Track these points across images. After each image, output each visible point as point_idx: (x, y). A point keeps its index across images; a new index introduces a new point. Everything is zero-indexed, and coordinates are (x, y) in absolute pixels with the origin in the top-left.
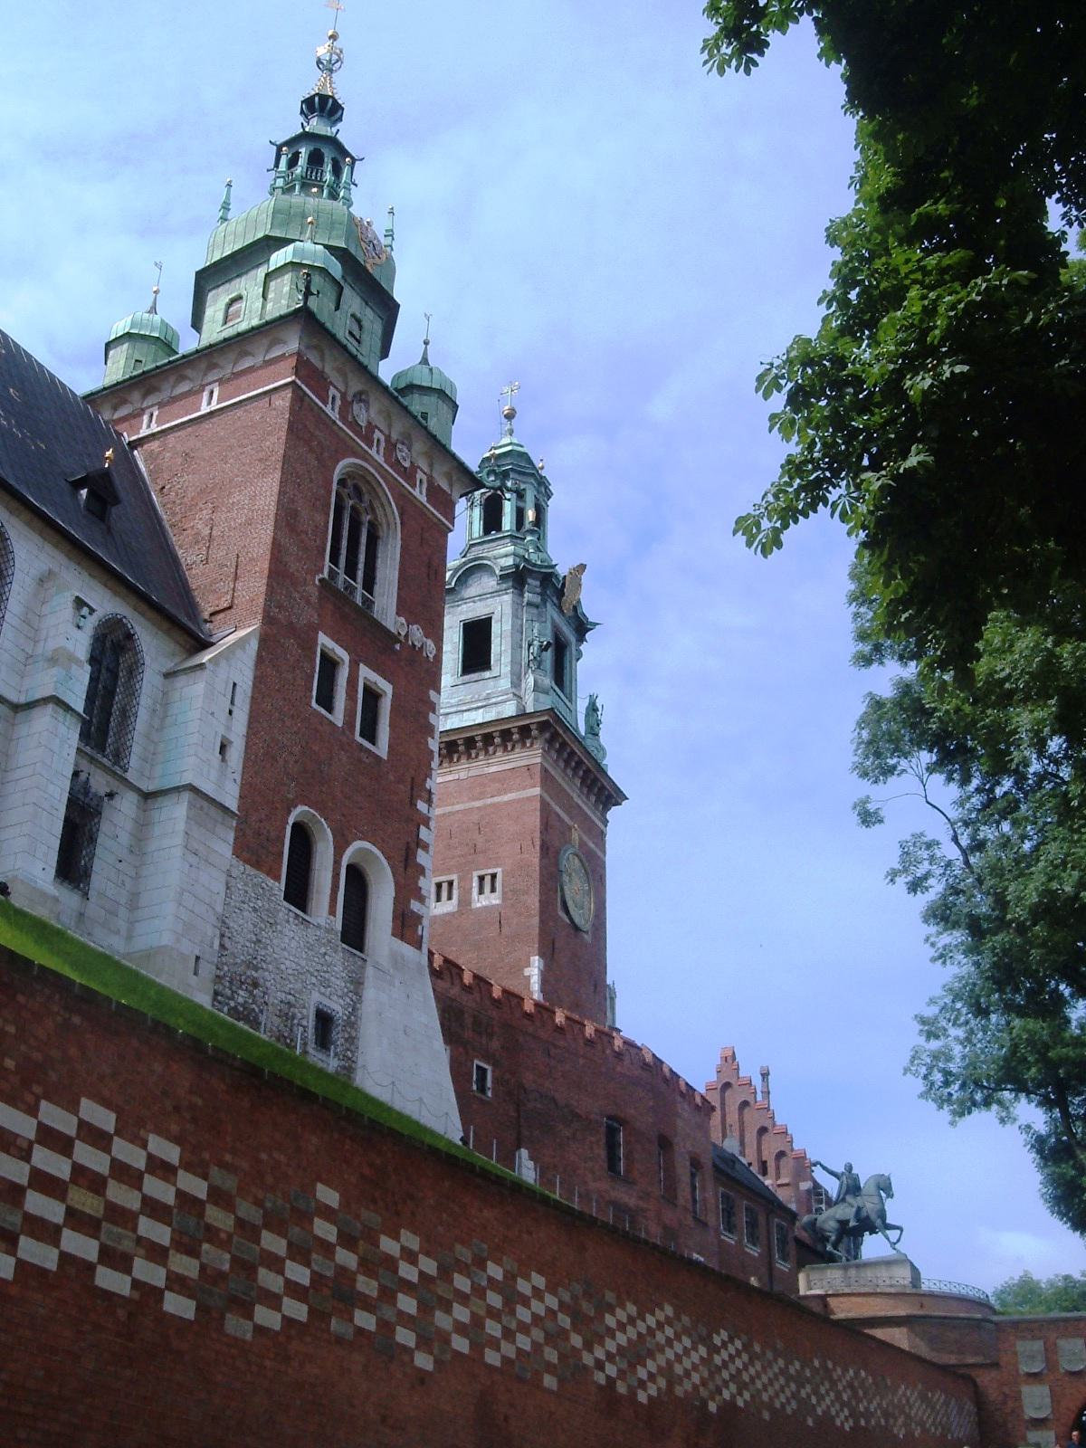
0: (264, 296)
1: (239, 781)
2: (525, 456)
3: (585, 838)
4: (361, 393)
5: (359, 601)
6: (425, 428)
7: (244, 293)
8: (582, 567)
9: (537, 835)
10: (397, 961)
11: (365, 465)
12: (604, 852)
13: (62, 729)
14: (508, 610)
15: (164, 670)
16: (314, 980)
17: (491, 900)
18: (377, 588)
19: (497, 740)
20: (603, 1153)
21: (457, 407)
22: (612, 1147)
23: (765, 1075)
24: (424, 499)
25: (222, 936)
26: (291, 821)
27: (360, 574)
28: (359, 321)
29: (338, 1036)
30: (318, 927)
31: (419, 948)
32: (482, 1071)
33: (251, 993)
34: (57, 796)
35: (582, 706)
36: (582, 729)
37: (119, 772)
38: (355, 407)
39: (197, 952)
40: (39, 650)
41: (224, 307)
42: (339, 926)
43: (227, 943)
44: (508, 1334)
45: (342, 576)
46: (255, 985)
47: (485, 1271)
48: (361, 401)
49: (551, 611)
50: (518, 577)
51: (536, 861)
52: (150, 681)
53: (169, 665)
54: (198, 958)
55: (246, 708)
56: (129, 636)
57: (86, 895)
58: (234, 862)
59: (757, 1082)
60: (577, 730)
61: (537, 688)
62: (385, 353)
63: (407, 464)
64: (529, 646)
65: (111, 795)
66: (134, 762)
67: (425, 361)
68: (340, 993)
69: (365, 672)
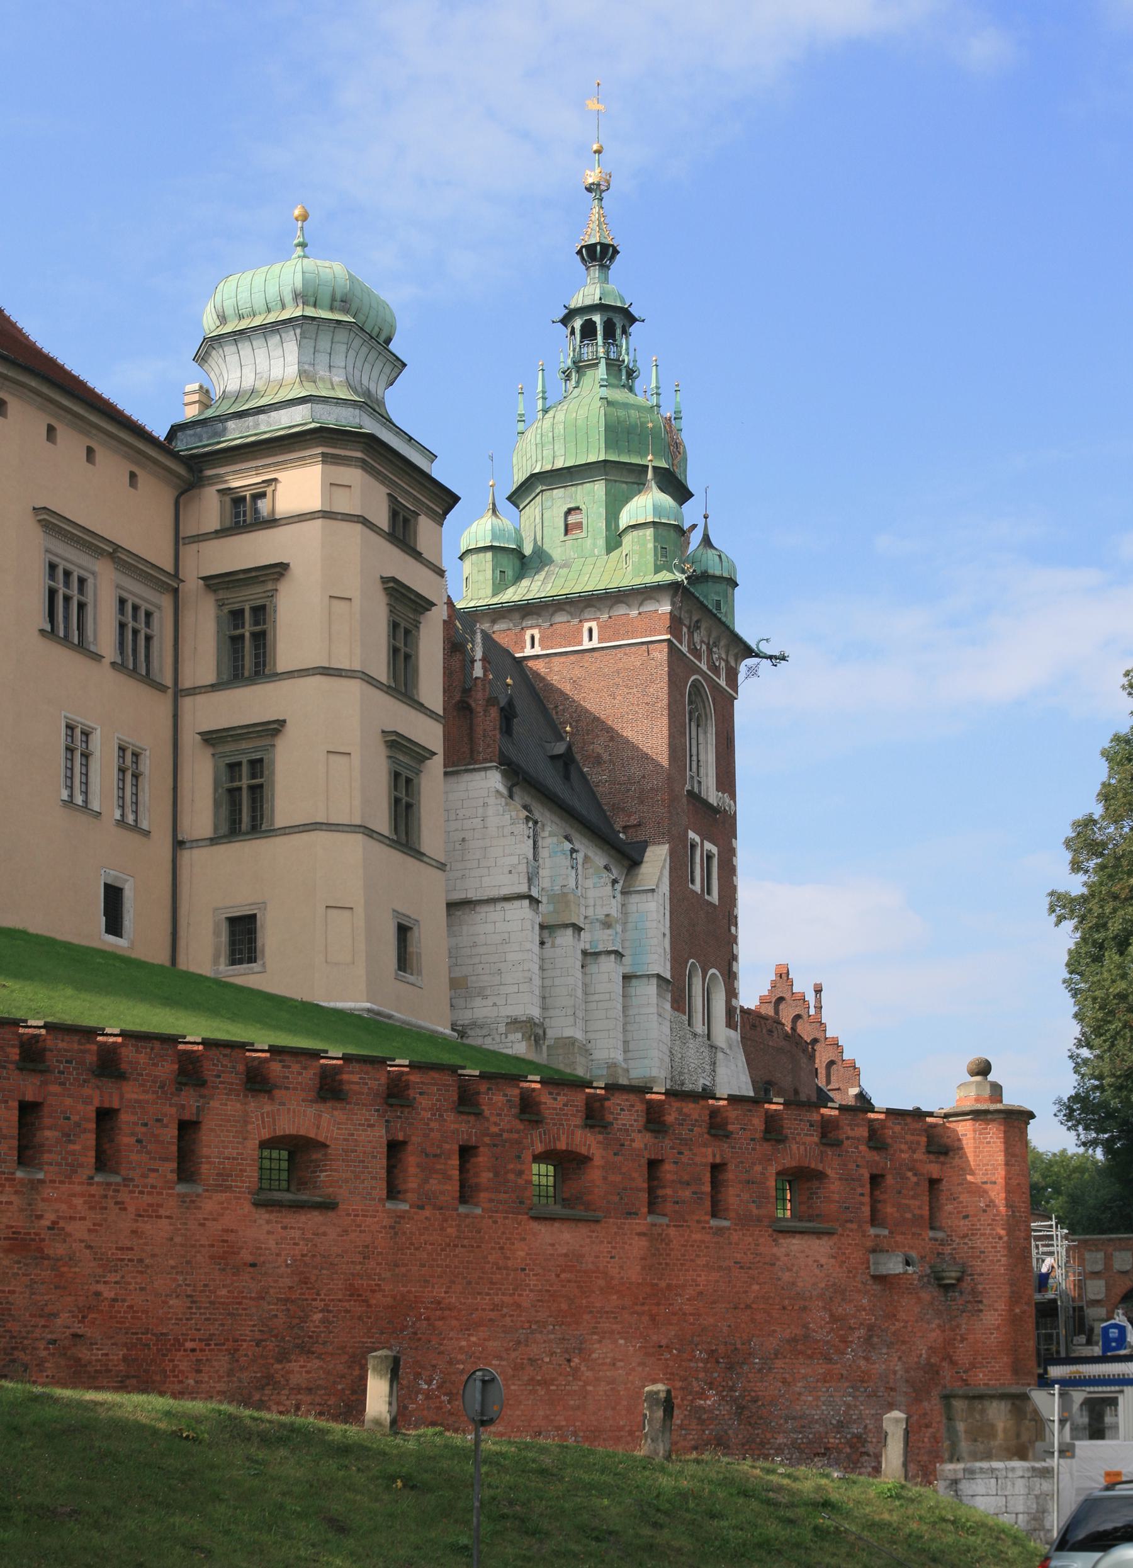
7: (583, 507)
23: (818, 991)
41: (563, 515)
59: (811, 997)
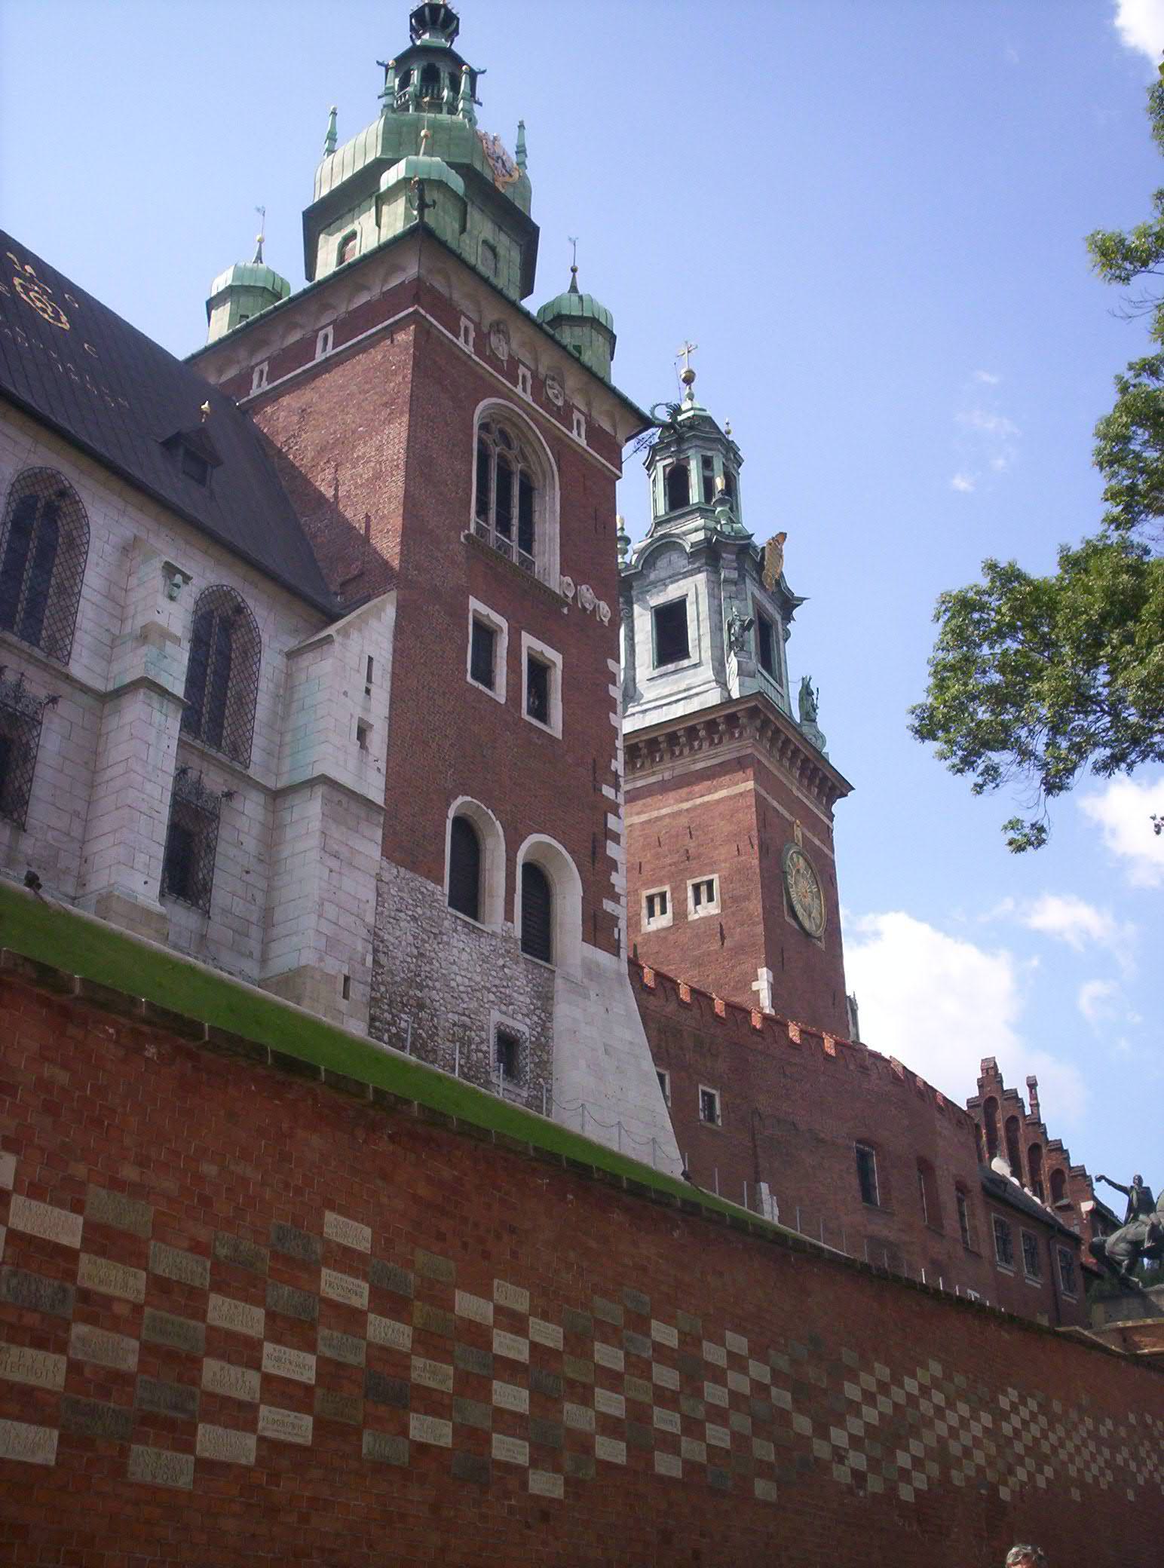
0: (378, 224)
1: (384, 771)
2: (709, 421)
3: (809, 835)
4: (498, 323)
5: (515, 559)
6: (578, 360)
8: (783, 536)
9: (755, 833)
10: (592, 971)
11: (511, 405)
12: (833, 851)
13: (157, 717)
14: (703, 591)
15: (286, 650)
16: (492, 997)
17: (710, 909)
18: (536, 546)
19: (702, 733)
20: (855, 1182)
21: (614, 337)
22: (864, 1173)
23: (1032, 1085)
24: (583, 442)
25: (375, 951)
26: (451, 814)
27: (515, 530)
28: (493, 249)
29: (527, 1063)
30: (493, 935)
31: (618, 955)
32: (709, 1099)
33: (416, 1016)
34: (157, 794)
35: (794, 691)
36: (797, 716)
37: (239, 767)
38: (493, 338)
39: (346, 972)
40: (127, 629)
42: (517, 932)
43: (383, 959)
44: (693, 1427)
45: (494, 533)
46: (421, 1006)
47: (648, 1335)
48: (499, 331)
49: (751, 587)
50: (710, 554)
51: (756, 862)
52: (270, 663)
53: (292, 643)
54: (347, 979)
55: (387, 685)
56: (239, 610)
57: (206, 914)
58: (385, 864)
59: (1024, 1094)
60: (791, 717)
61: (741, 672)
62: (527, 289)
63: (560, 403)
64: (730, 626)
65: (229, 795)
66: (256, 755)
67: (574, 289)
68: (525, 1011)
69: (528, 640)
